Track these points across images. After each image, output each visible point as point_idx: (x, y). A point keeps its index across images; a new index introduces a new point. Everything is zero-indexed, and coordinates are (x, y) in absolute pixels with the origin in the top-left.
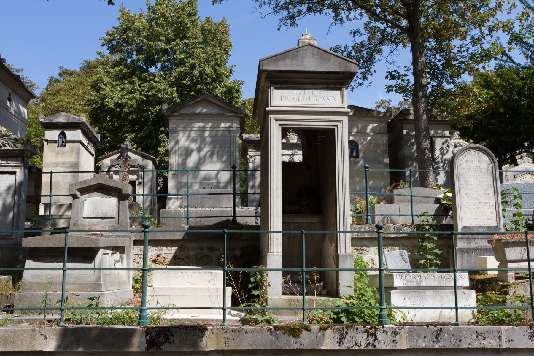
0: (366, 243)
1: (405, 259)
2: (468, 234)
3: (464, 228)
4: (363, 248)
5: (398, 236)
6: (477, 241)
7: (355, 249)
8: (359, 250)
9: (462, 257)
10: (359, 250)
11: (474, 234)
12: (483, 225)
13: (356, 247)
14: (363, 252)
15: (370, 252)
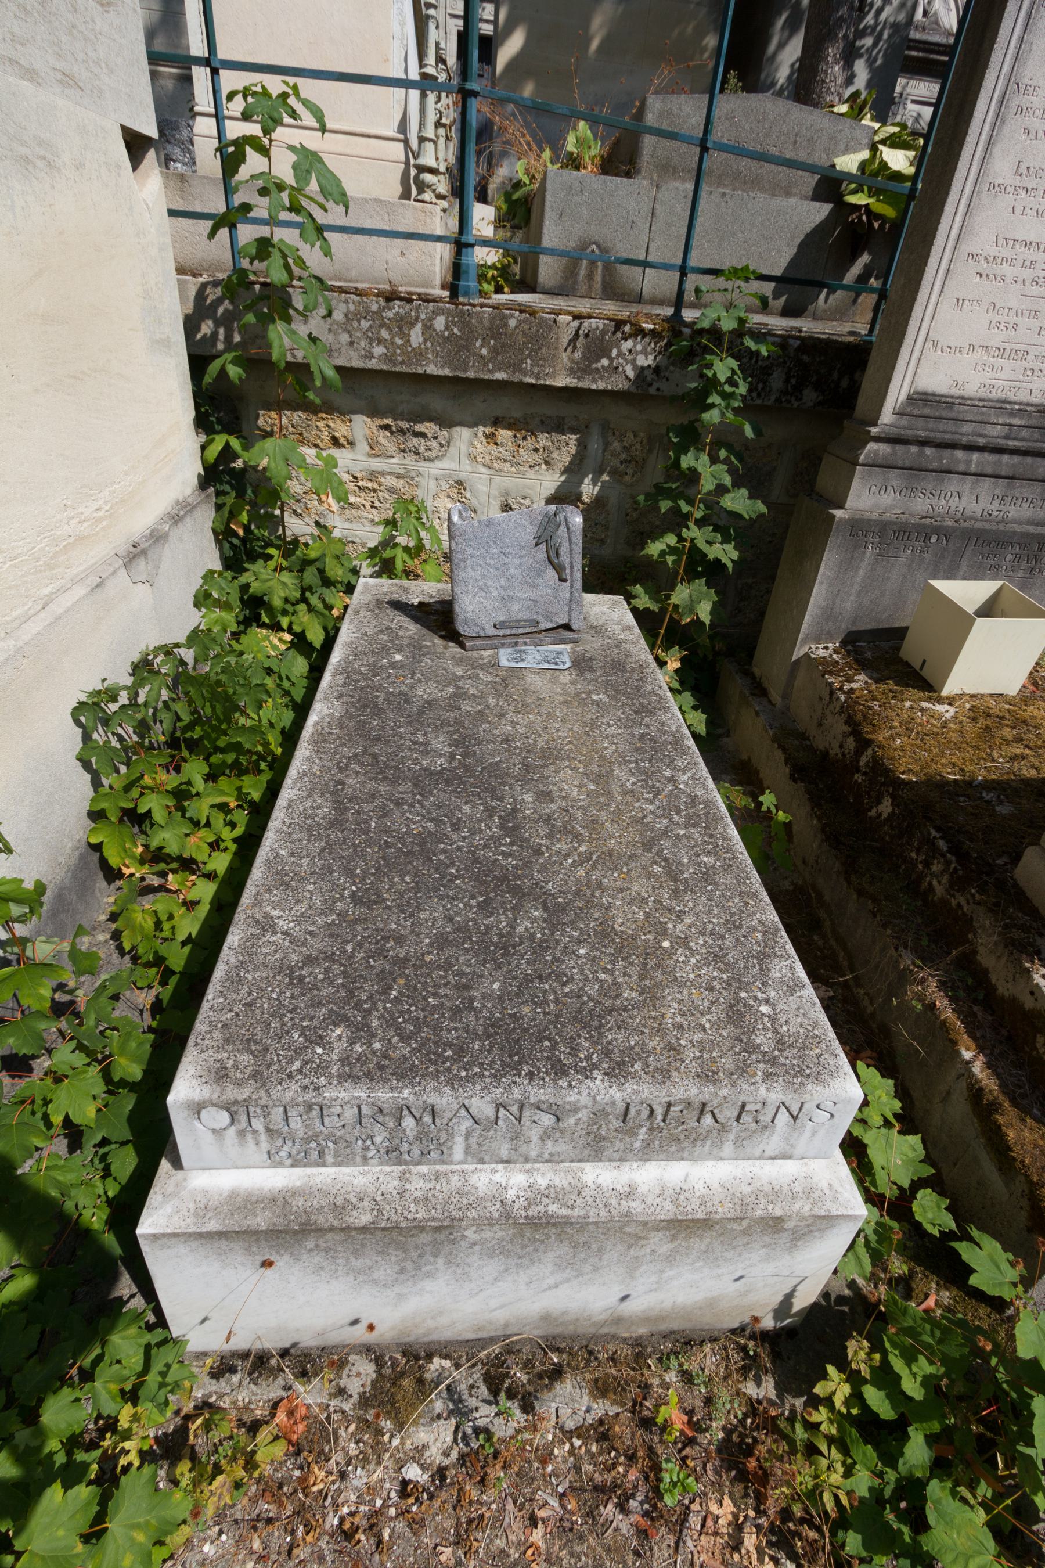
0: (436, 402)
1: (565, 559)
2: (923, 443)
3: (921, 399)
4: (420, 428)
5: (584, 384)
6: (953, 484)
7: (387, 427)
8: (402, 432)
9: (848, 564)
10: (402, 432)
11: (953, 446)
12: (1023, 396)
13: (388, 421)
14: (420, 444)
15: (453, 450)
